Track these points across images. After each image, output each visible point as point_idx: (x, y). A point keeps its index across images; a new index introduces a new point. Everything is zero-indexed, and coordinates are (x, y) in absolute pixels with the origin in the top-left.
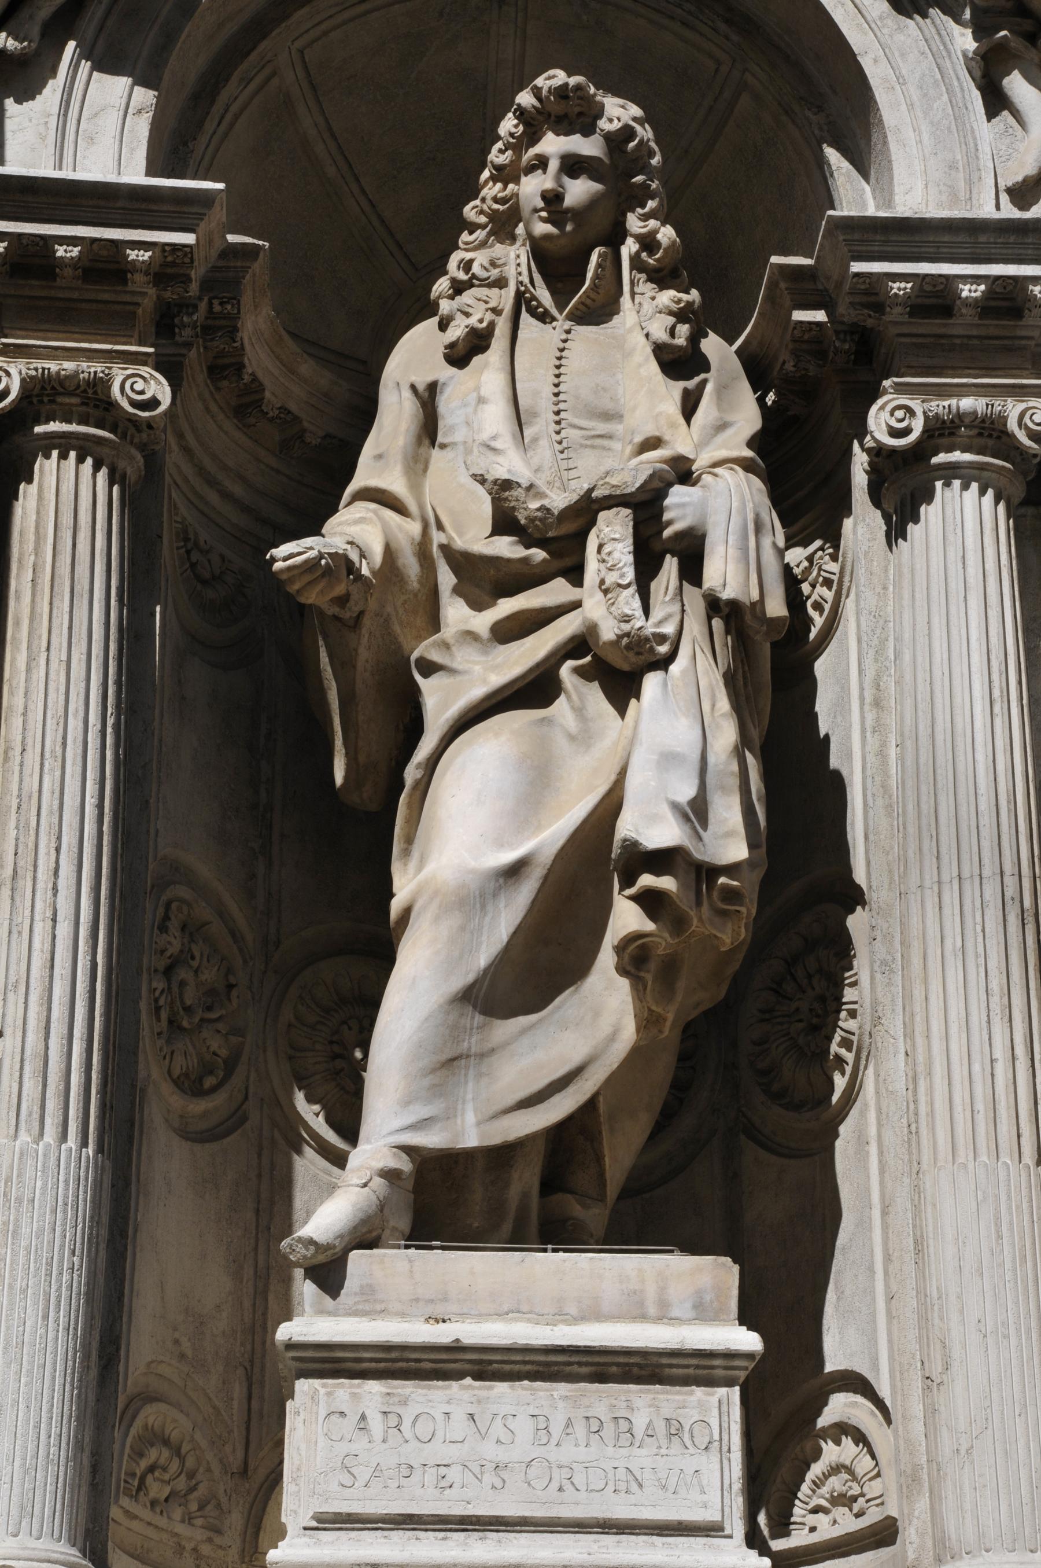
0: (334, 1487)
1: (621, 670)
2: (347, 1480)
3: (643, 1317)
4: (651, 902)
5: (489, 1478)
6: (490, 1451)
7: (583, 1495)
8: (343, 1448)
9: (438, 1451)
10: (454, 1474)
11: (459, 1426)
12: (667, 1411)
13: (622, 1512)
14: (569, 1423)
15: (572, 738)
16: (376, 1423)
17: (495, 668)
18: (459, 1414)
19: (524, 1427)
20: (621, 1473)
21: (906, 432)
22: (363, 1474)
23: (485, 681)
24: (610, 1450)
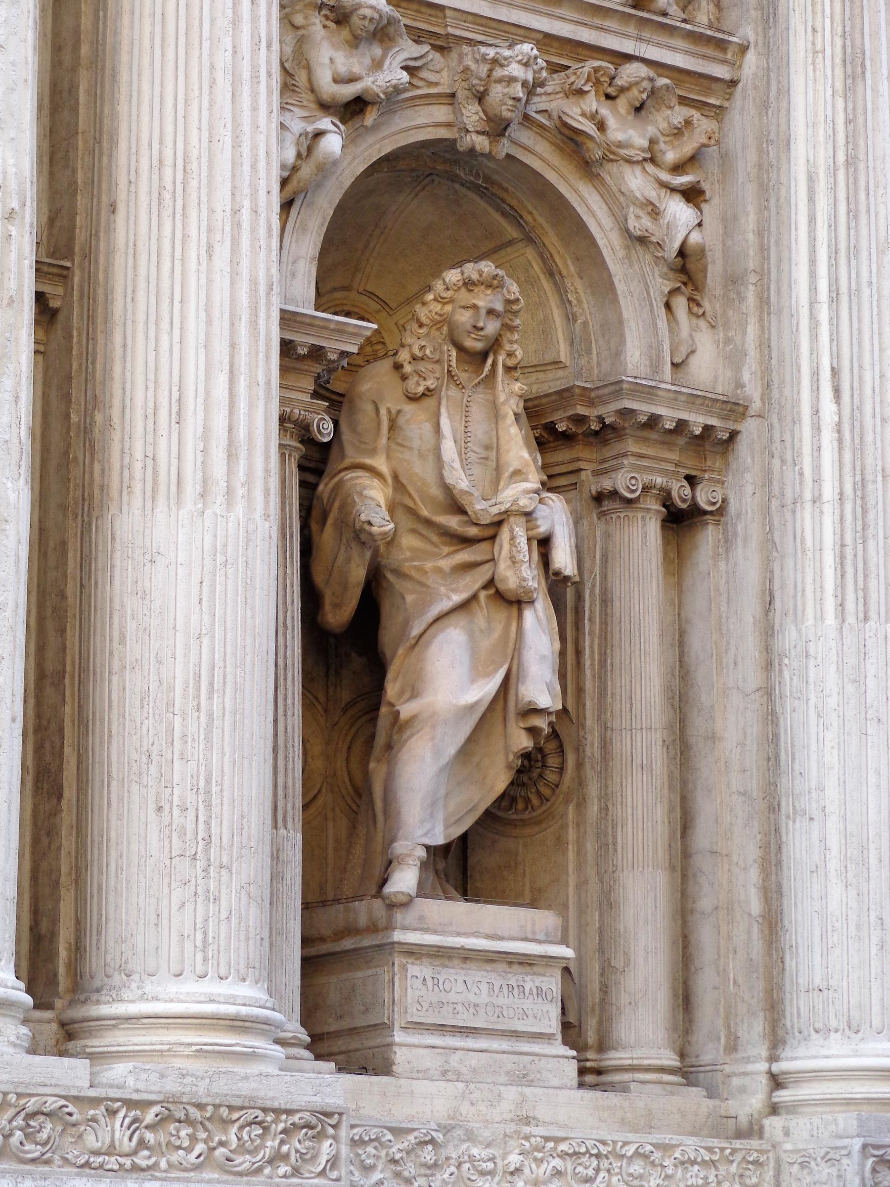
0: (415, 1011)
1: (515, 603)
2: (419, 1008)
3: (525, 939)
4: (532, 731)
5: (472, 1010)
6: (472, 998)
7: (506, 1020)
8: (418, 993)
9: (452, 997)
10: (459, 1008)
11: (461, 986)
12: (537, 984)
13: (520, 1027)
14: (501, 987)
15: (481, 631)
16: (429, 983)
17: (455, 591)
18: (460, 981)
19: (484, 987)
20: (521, 1012)
21: (633, 491)
22: (425, 1005)
23: (449, 598)
24: (516, 1000)
